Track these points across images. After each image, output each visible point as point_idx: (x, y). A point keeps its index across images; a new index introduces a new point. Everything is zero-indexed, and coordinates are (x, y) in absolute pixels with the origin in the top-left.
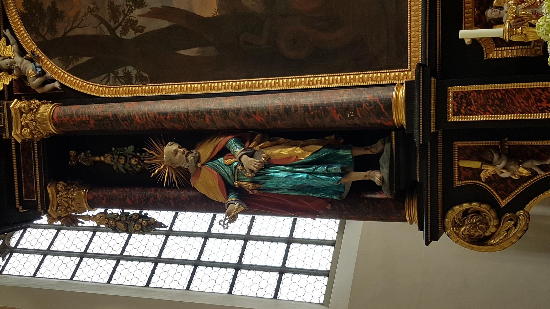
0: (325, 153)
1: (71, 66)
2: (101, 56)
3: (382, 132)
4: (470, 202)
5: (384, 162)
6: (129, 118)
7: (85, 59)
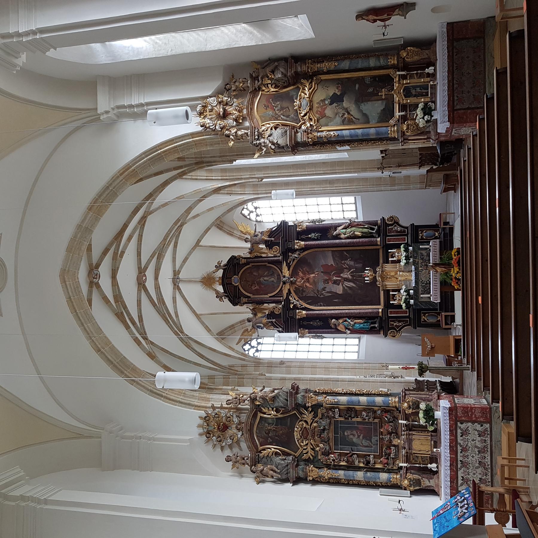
2: (315, 300)
3: (377, 317)
5: (377, 322)
6: (325, 314)
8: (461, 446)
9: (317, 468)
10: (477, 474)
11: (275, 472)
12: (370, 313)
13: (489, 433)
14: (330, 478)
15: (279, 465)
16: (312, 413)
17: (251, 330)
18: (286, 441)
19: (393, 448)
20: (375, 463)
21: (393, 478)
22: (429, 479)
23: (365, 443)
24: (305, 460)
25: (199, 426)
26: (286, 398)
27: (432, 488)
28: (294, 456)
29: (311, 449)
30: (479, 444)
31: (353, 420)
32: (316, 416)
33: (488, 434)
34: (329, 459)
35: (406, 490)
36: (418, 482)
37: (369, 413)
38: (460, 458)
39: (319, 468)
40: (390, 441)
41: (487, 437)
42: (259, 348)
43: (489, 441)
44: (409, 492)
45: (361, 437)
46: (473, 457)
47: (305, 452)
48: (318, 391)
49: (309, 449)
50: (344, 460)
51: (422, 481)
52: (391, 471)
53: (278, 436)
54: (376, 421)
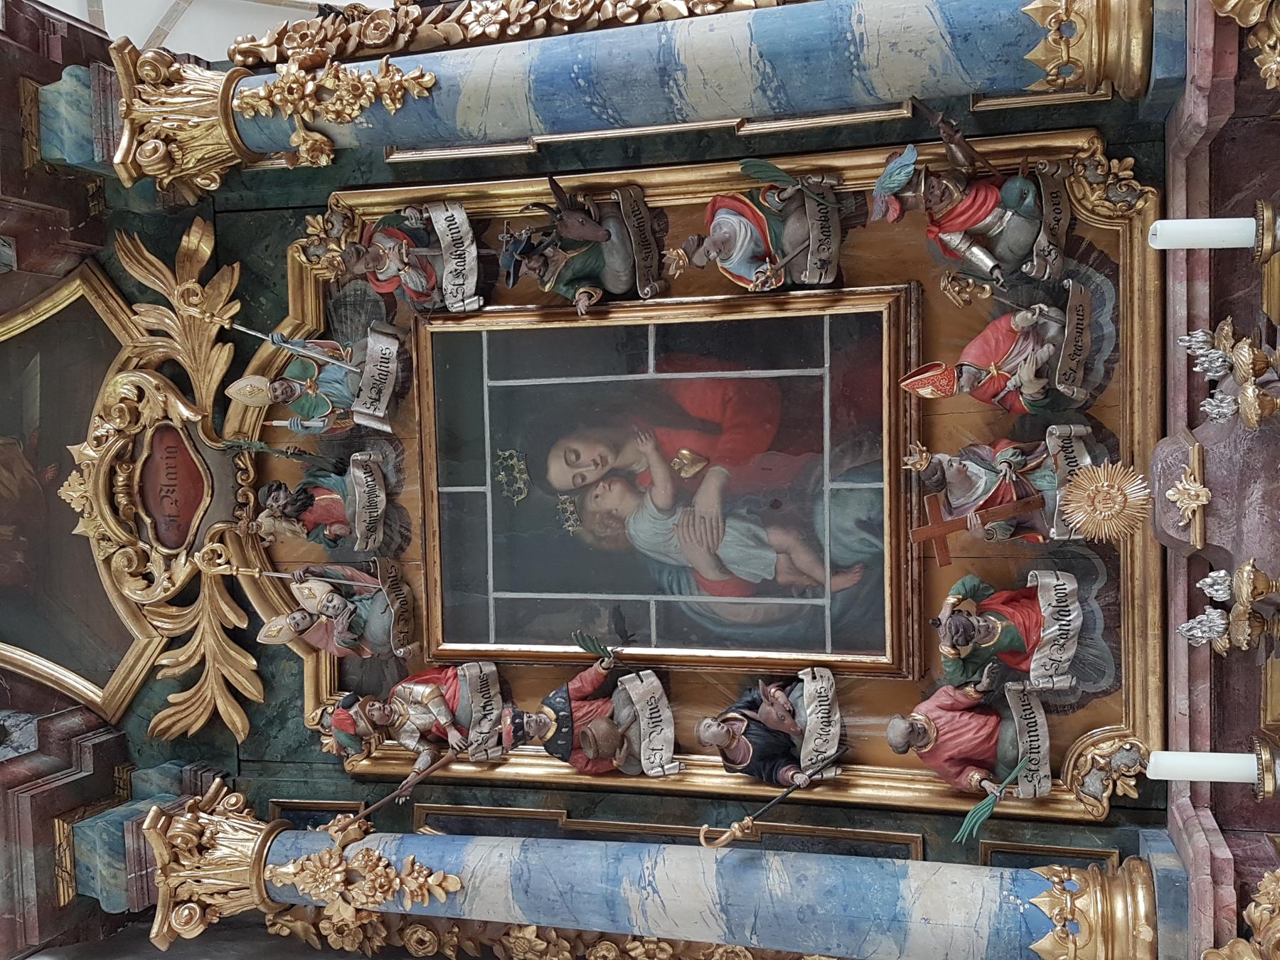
16: (228, 280)
19: (1051, 585)
20: (847, 757)
21: (1070, 923)
23: (751, 550)
29: (234, 635)
31: (623, 317)
32: (259, 300)
34: (387, 729)
40: (1022, 511)
45: (708, 498)
47: (175, 662)
49: (207, 641)
50: (521, 736)
52: (1029, 838)
54: (864, 302)
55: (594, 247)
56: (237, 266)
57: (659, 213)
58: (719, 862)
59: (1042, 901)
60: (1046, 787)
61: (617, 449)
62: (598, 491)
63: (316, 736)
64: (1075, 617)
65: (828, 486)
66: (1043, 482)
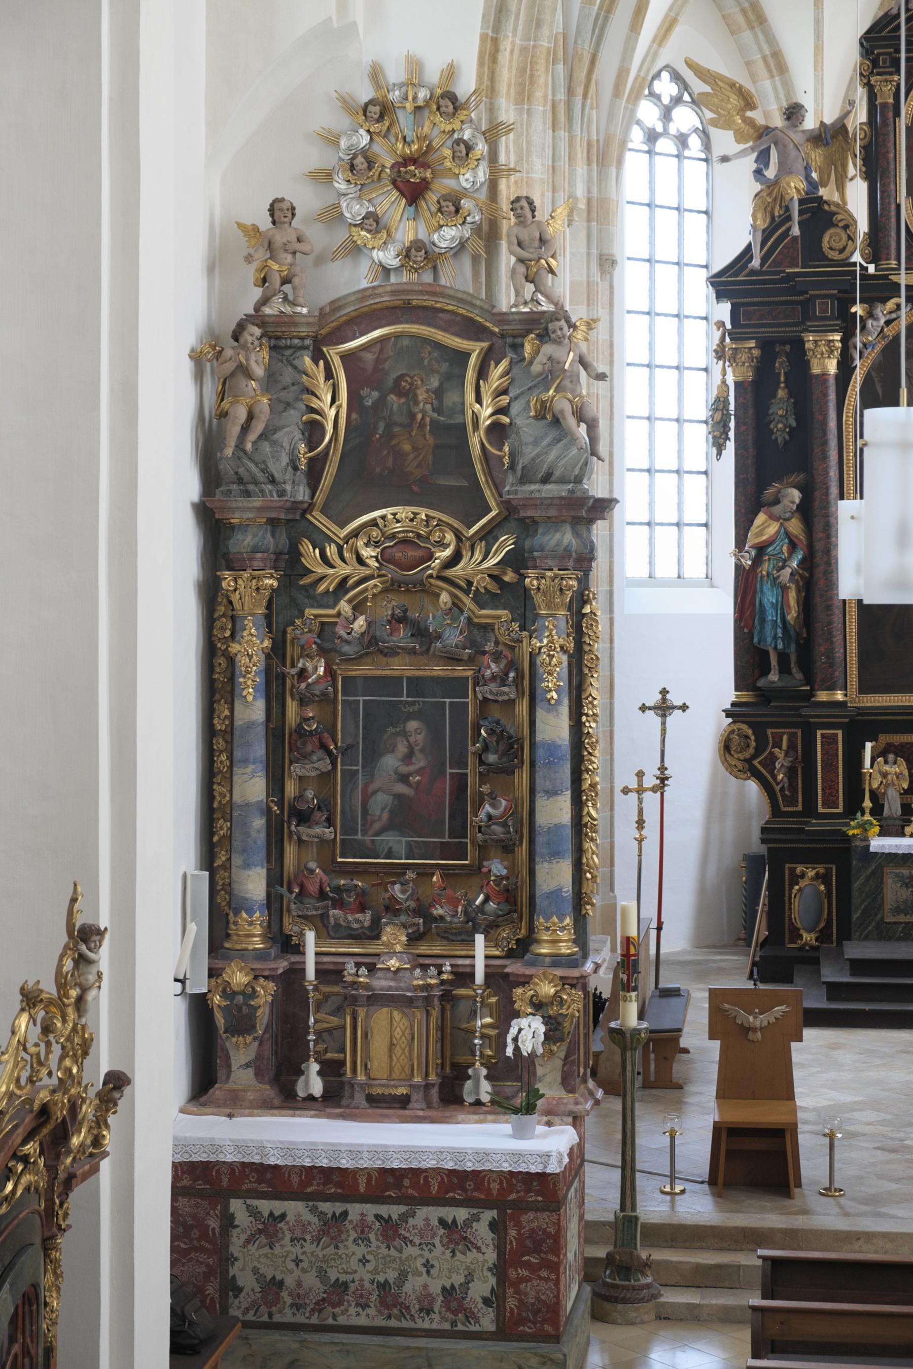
0: (792, 633)
1: (874, 374)
4: (756, 741)
6: (825, 457)
7: (880, 390)
8: (404, 1217)
9: (270, 602)
10: (297, 1273)
11: (246, 429)
12: (830, 654)
13: (460, 1327)
14: (231, 660)
15: (274, 443)
17: (750, 122)
18: (369, 466)
19: (366, 918)
20: (300, 841)
21: (251, 923)
22: (257, 1066)
23: (381, 803)
24: (295, 555)
25: (415, 66)
26: (557, 473)
27: (221, 1073)
28: (311, 507)
29: (345, 580)
30: (413, 1286)
33: (454, 1323)
35: (210, 976)
36: (241, 1023)
37: (505, 825)
38: (355, 1210)
39: (268, 617)
40: (392, 909)
41: (443, 1319)
42: (665, 145)
43: (426, 1325)
44: (204, 990)
45: (402, 789)
46: (364, 1261)
47: (331, 551)
48: (587, 610)
51: (249, 1039)
53: (389, 435)
55: (496, 752)
56: (499, 592)
57: (513, 773)
58: (262, 801)
59: (257, 914)
60: (294, 913)
61: (421, 751)
62: (405, 742)
63: (301, 615)
64: (355, 926)
65: (404, 839)
66: (403, 918)
